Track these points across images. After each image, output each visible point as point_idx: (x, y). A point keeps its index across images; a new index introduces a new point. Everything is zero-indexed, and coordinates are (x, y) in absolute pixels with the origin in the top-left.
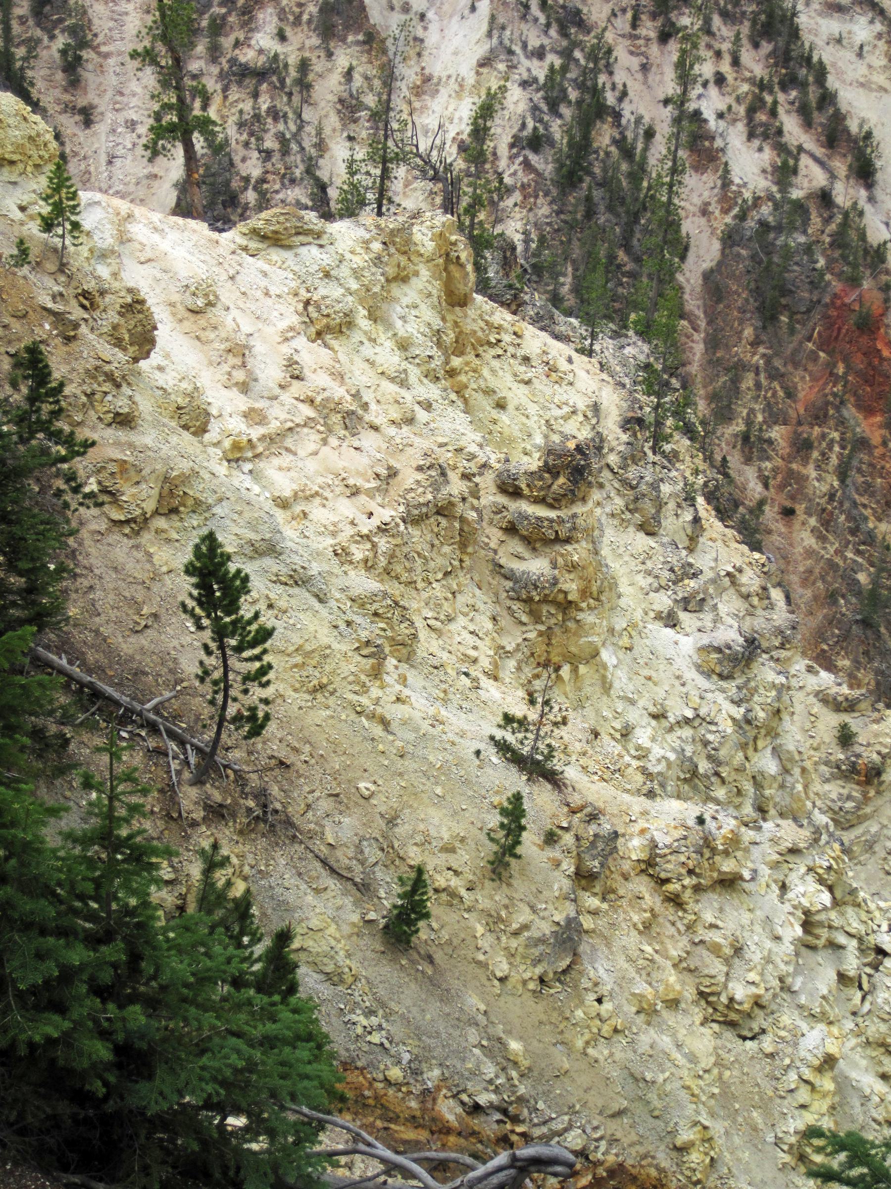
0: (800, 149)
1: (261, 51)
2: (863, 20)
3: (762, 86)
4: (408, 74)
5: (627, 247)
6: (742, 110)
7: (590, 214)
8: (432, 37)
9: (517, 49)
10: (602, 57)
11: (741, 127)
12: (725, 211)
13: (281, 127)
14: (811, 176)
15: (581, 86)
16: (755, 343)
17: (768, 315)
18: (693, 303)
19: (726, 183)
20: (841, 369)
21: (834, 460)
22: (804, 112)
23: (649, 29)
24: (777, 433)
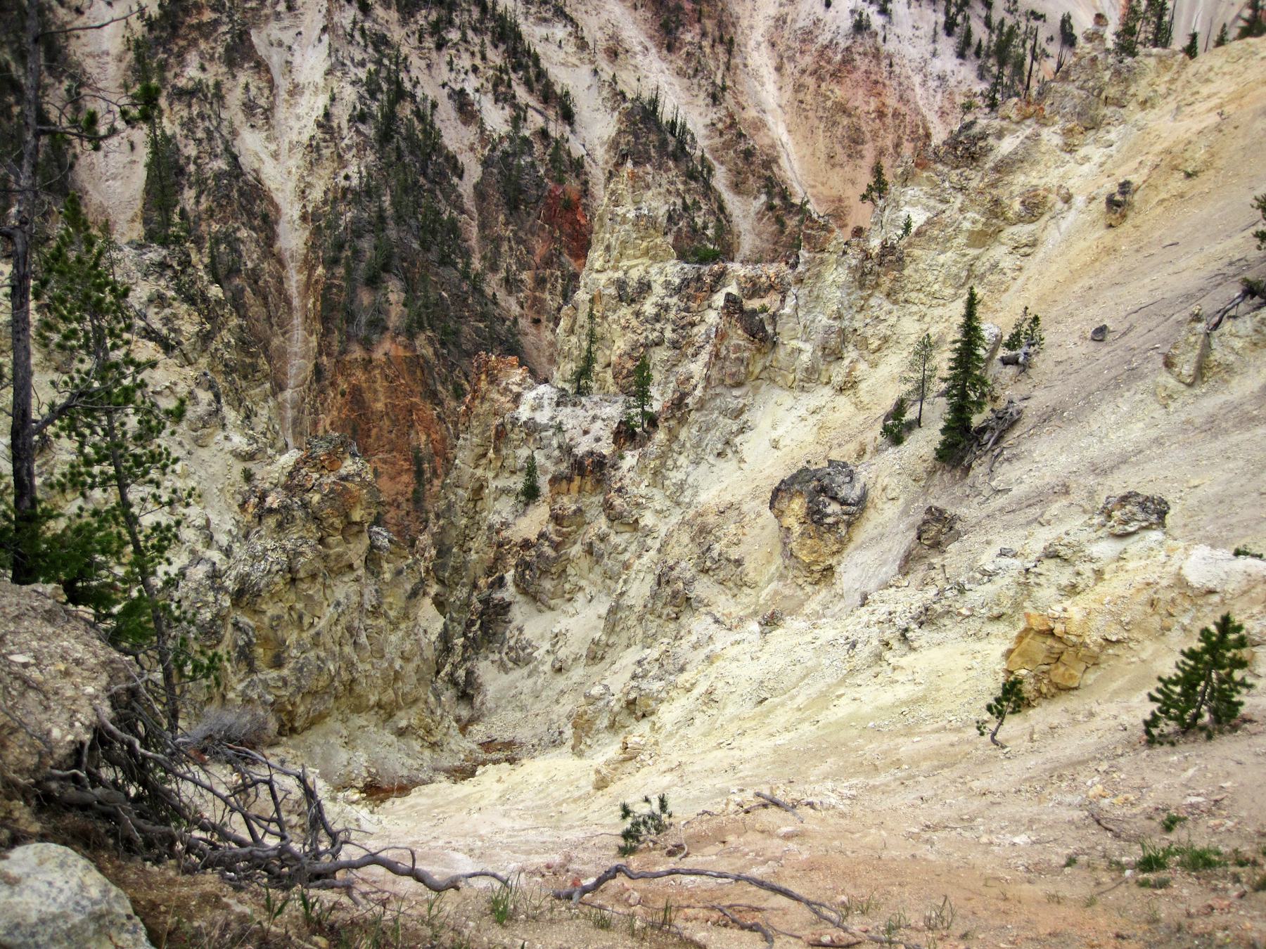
0: (527, 105)
1: (191, 79)
2: (560, 26)
3: (501, 70)
4: (283, 84)
5: (425, 174)
6: (490, 86)
7: (399, 157)
8: (297, 60)
9: (348, 62)
10: (403, 64)
11: (490, 95)
12: (483, 148)
13: (207, 123)
14: (535, 121)
15: (388, 80)
16: (507, 224)
17: (513, 205)
18: (469, 203)
19: (483, 131)
20: (557, 234)
21: (559, 288)
22: (528, 84)
23: (429, 43)
24: (526, 276)
